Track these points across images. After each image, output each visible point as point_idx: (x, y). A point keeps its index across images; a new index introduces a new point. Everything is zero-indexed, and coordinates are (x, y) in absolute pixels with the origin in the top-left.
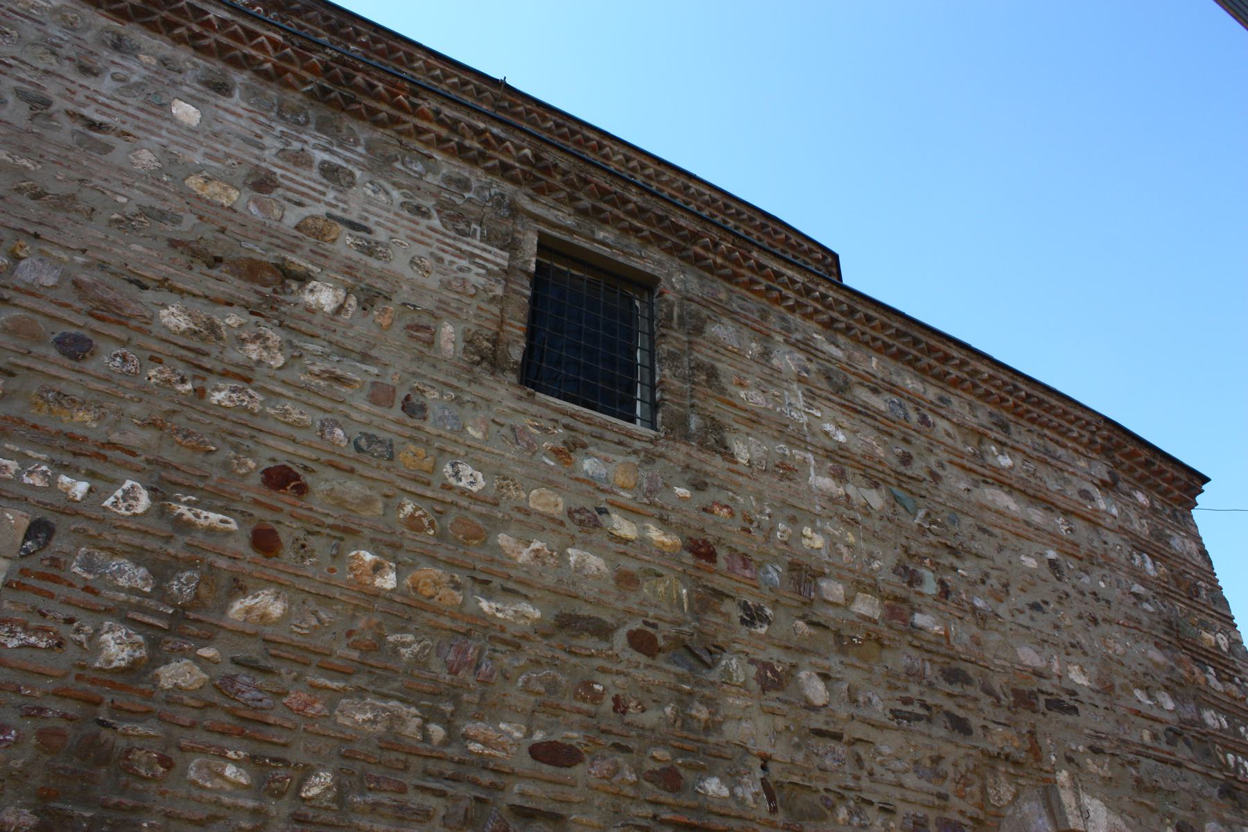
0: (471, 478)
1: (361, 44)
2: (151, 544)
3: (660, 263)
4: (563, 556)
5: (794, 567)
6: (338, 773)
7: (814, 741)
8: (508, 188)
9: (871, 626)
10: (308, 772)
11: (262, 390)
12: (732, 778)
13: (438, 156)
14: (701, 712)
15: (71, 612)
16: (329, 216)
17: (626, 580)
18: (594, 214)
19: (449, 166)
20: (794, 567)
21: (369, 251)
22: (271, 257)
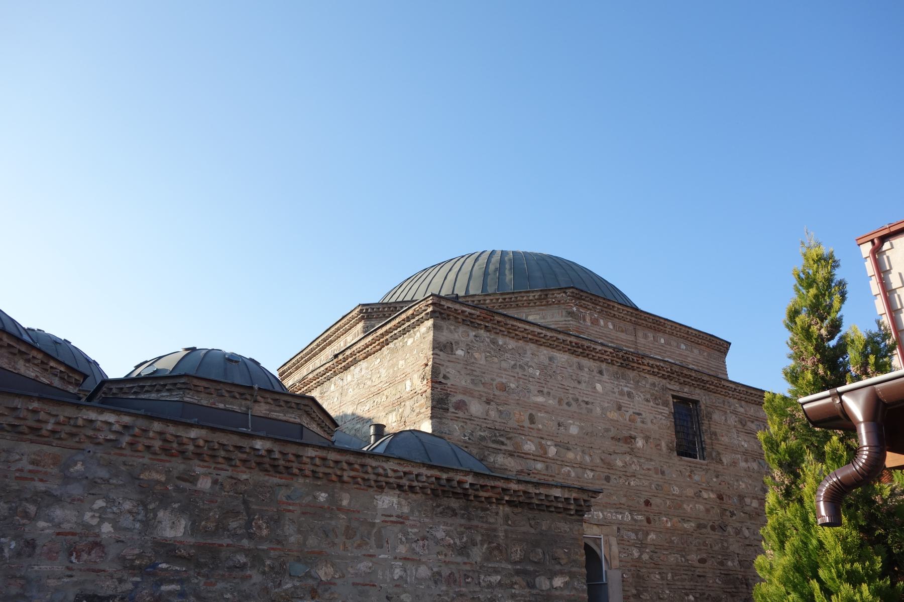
0: (676, 490)
1: (600, 306)
2: (634, 527)
3: (699, 394)
4: (695, 506)
5: (739, 496)
6: (672, 573)
7: (747, 547)
8: (664, 381)
9: (757, 510)
10: (667, 574)
11: (638, 478)
12: (733, 561)
13: (648, 376)
14: (725, 544)
15: (627, 547)
16: (634, 413)
17: (708, 511)
18: (685, 383)
19: (651, 379)
20: (739, 496)
21: (643, 422)
22: (627, 435)
